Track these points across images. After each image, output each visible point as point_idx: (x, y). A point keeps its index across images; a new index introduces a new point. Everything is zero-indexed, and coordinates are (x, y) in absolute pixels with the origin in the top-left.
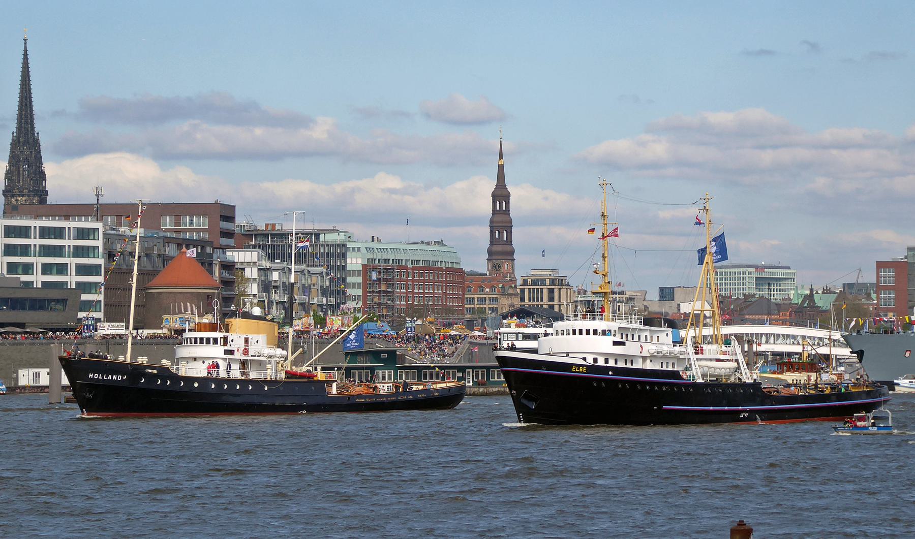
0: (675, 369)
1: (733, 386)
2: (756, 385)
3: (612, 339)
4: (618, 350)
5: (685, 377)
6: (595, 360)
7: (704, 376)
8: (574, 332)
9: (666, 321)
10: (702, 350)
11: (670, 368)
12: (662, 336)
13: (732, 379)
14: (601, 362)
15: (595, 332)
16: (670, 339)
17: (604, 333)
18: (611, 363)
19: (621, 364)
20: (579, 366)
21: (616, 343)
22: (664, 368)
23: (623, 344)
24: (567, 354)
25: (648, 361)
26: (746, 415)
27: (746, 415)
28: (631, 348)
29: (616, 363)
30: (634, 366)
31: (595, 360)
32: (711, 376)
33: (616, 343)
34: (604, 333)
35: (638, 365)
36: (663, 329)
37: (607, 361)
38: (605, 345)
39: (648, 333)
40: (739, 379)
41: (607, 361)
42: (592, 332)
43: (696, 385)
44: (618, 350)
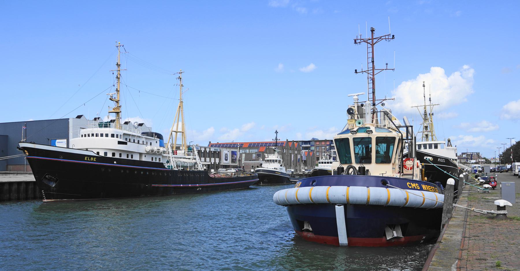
1: (194, 172)
3: (116, 140)
4: (122, 147)
5: (166, 167)
6: (106, 154)
7: (178, 166)
9: (156, 134)
11: (158, 161)
12: (154, 143)
13: (193, 169)
14: (110, 155)
15: (107, 135)
17: (113, 136)
18: (117, 156)
19: (124, 157)
21: (120, 143)
22: (154, 161)
23: (126, 143)
24: (87, 150)
25: (143, 156)
28: (130, 147)
29: (120, 155)
30: (134, 159)
31: (106, 154)
33: (120, 143)
34: (113, 136)
35: (136, 158)
39: (144, 140)
41: (114, 154)
42: (104, 135)
43: (172, 172)
44: (122, 147)
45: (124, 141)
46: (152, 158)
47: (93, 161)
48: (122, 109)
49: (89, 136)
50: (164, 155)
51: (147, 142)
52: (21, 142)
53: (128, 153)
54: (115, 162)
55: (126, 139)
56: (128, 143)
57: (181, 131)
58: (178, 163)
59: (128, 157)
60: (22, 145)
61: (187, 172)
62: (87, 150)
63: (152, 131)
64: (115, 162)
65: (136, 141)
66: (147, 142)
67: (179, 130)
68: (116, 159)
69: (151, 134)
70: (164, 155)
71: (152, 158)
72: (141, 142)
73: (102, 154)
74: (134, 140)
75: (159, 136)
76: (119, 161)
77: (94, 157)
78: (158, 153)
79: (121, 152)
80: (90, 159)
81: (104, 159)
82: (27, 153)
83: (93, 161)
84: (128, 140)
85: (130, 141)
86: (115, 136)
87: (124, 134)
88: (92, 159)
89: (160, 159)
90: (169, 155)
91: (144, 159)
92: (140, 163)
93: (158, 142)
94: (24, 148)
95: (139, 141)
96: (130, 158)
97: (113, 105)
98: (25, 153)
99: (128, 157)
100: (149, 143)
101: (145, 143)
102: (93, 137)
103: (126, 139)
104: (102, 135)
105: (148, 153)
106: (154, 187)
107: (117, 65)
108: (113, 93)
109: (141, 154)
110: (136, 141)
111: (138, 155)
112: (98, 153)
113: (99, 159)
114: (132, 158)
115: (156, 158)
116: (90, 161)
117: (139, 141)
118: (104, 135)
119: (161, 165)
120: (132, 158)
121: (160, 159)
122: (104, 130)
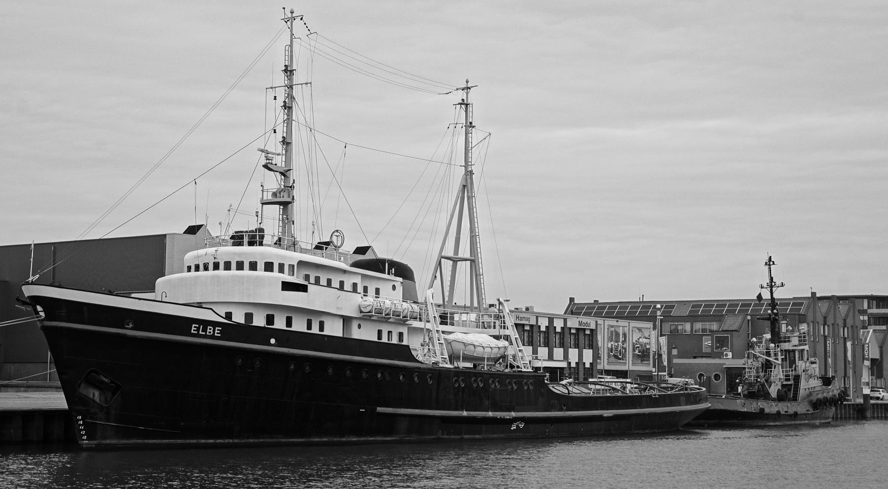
0: (405, 343)
1: (500, 376)
2: (537, 376)
4: (294, 299)
6: (249, 317)
7: (453, 357)
8: (216, 266)
9: (392, 264)
10: (452, 318)
11: (395, 340)
12: (386, 288)
13: (499, 367)
14: (259, 321)
15: (253, 266)
17: (269, 267)
18: (280, 324)
19: (299, 326)
20: (205, 323)
21: (287, 286)
22: (385, 339)
23: (303, 288)
24: (199, 305)
25: (355, 325)
27: (522, 426)
28: (316, 298)
29: (289, 322)
30: (327, 332)
31: (249, 317)
32: (466, 358)
33: (287, 286)
34: (269, 267)
35: (334, 329)
36: (385, 276)
37: (270, 319)
38: (268, 290)
39: (358, 280)
40: (512, 366)
41: (270, 319)
42: (246, 265)
43: (436, 373)
44: (294, 299)
45: (301, 281)
46: (380, 333)
47: (213, 337)
48: (299, 194)
49: (206, 268)
50: (416, 324)
51: (365, 289)
52: (28, 283)
53: (309, 314)
54: (273, 341)
55: (307, 277)
56: (309, 286)
57: (468, 256)
58: (457, 347)
59: (309, 327)
60: (29, 291)
61: (482, 374)
62: (199, 305)
63: (381, 256)
64: (273, 341)
65: (336, 284)
66: (365, 289)
67: (460, 255)
68: (277, 333)
69: (377, 265)
70: (416, 324)
71: (380, 333)
72: (348, 286)
73: (239, 318)
74: (329, 282)
75: (403, 271)
76: (287, 337)
77: (214, 324)
78: (401, 319)
79: (291, 312)
80: (205, 330)
81: (246, 331)
82: (42, 314)
83: (213, 337)
84: (312, 280)
85: (317, 281)
86: (276, 267)
87: (301, 263)
88: (210, 329)
89: (401, 335)
90: (428, 326)
92: (345, 344)
93: (399, 289)
94: (37, 300)
95: (342, 283)
96: (315, 330)
97: (273, 182)
98: (37, 313)
99: (309, 327)
100: (371, 291)
101: (360, 289)
102: (216, 272)
103: (307, 277)
104: (240, 266)
105: (366, 317)
107: (286, 71)
108: (275, 145)
109: (347, 320)
110: (336, 284)
111: (339, 323)
112: (229, 316)
113: (230, 329)
114: (322, 328)
115: (390, 332)
116: (205, 337)
117: (342, 283)
118: (246, 265)
119: (404, 352)
120: (322, 328)
121: (401, 335)
122: (246, 251)
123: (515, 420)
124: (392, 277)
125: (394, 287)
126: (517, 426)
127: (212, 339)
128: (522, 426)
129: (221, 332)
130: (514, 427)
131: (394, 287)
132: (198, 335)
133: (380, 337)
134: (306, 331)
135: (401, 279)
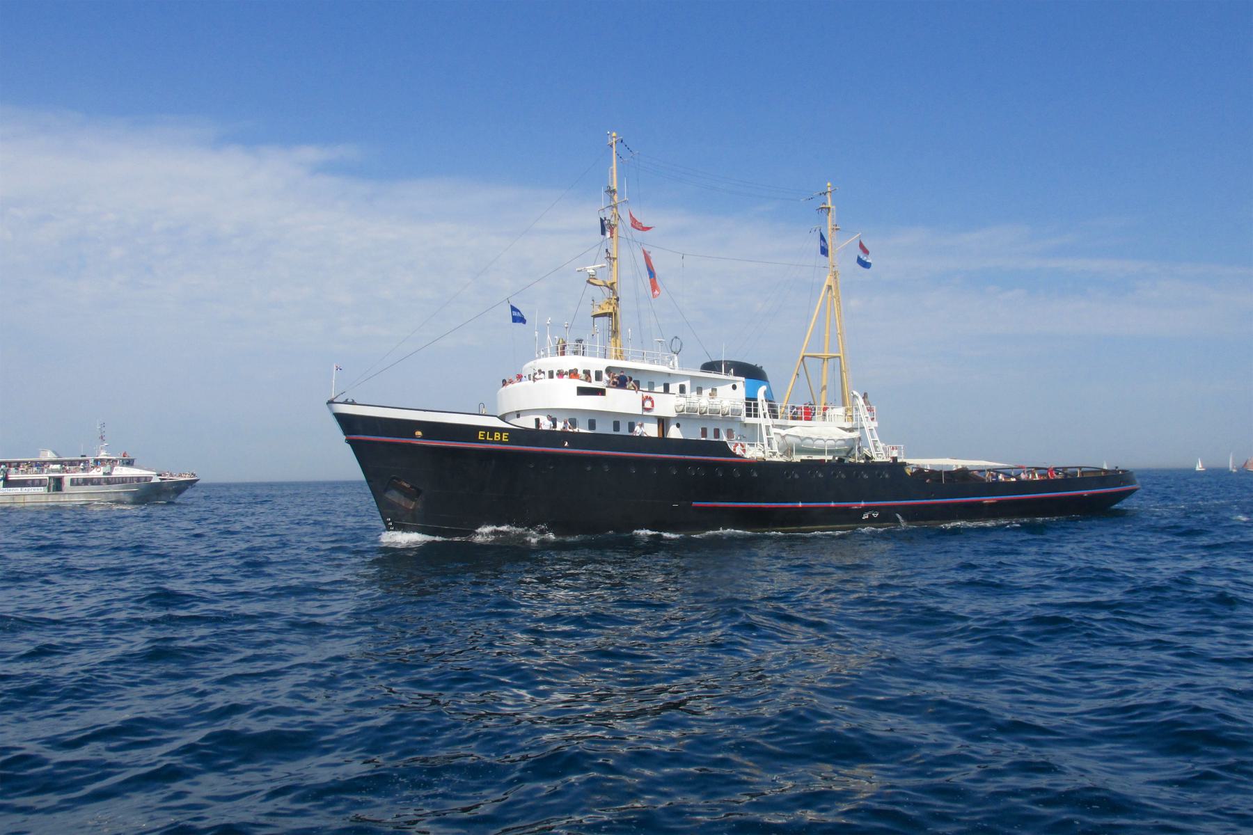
16: (741, 393)
18: (583, 429)
19: (604, 428)
20: (492, 430)
23: (601, 392)
26: (875, 515)
28: (623, 401)
29: (592, 424)
33: (582, 391)
34: (573, 374)
36: (722, 376)
37: (574, 423)
38: (565, 396)
40: (867, 458)
47: (501, 442)
56: (608, 390)
63: (714, 359)
68: (564, 435)
76: (576, 439)
77: (501, 430)
79: (593, 418)
80: (492, 436)
81: (552, 437)
88: (497, 436)
91: (674, 433)
92: (662, 443)
96: (624, 431)
106: (696, 507)
109: (663, 422)
113: (518, 435)
116: (493, 442)
119: (722, 448)
123: (866, 509)
124: (732, 377)
125: (734, 387)
126: (870, 516)
127: (500, 443)
128: (875, 515)
129: (508, 437)
130: (866, 517)
131: (734, 387)
132: (485, 441)
133: (704, 432)
134: (612, 432)
135: (743, 379)
